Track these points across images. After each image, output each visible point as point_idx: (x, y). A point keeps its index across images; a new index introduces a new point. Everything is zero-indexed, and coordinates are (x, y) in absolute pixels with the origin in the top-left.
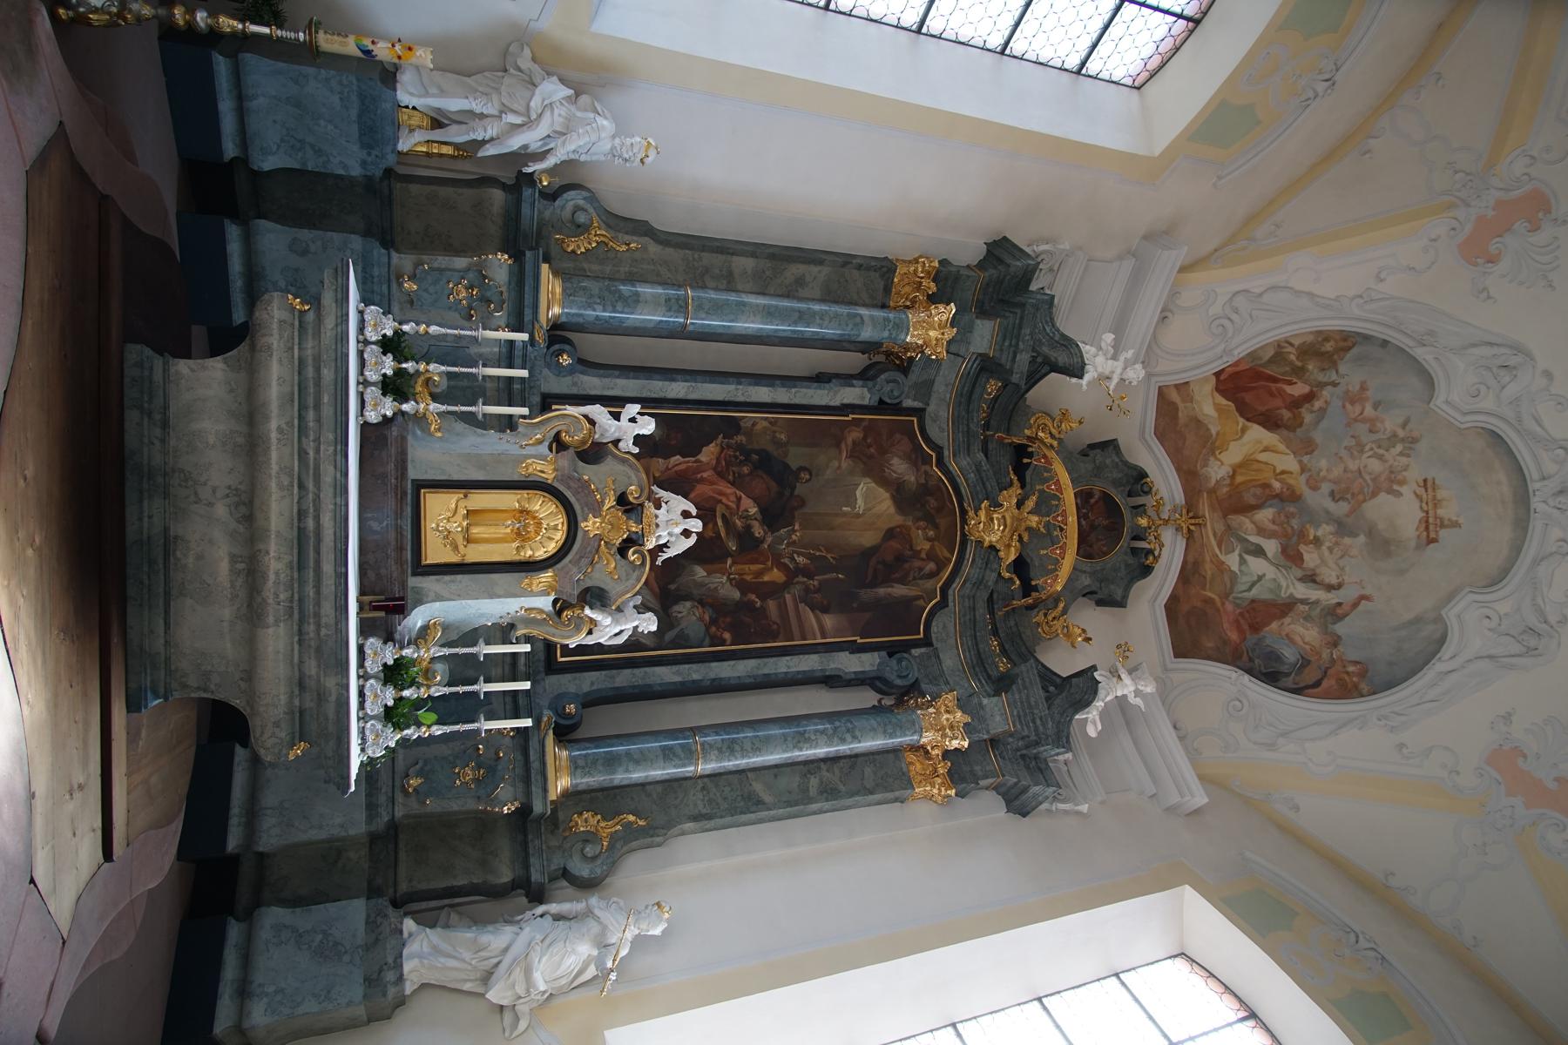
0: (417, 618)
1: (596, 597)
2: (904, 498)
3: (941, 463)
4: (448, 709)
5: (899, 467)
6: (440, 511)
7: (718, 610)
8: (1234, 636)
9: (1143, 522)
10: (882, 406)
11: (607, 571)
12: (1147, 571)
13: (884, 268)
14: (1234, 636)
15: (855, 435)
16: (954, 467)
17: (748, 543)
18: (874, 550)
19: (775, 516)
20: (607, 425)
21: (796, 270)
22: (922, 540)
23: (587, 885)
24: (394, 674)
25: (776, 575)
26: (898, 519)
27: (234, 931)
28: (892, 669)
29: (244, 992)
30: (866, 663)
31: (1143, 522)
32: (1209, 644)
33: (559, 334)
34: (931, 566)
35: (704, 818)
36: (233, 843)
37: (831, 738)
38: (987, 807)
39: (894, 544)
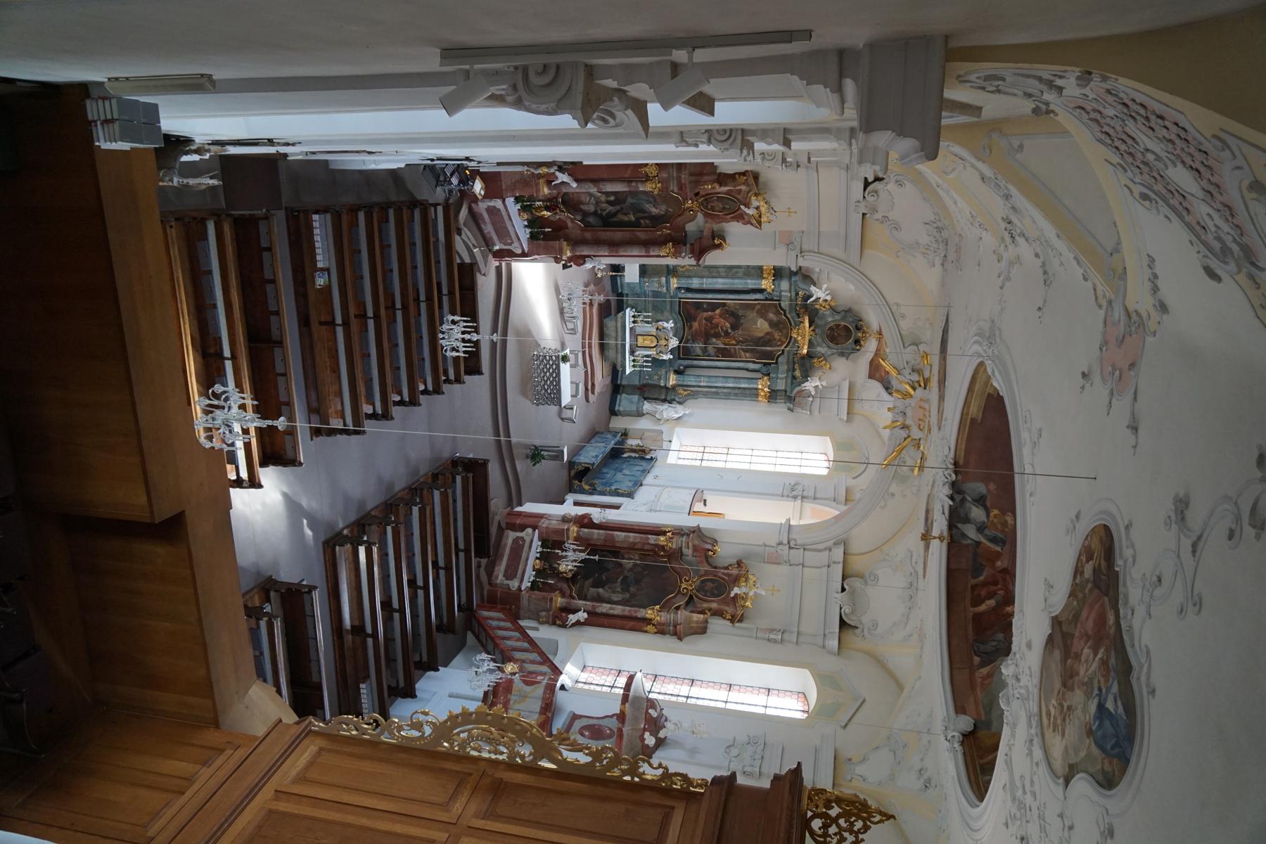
0: (637, 353)
1: (662, 353)
2: (772, 324)
3: (785, 315)
4: (641, 366)
5: (771, 316)
6: (640, 339)
7: (719, 349)
8: (883, 374)
9: (860, 335)
10: (766, 299)
11: (663, 349)
12: (858, 350)
13: (760, 268)
14: (883, 374)
15: (759, 307)
16: (789, 316)
17: (727, 334)
18: (762, 337)
19: (734, 327)
20: (665, 325)
21: (735, 270)
22: (777, 335)
23: (680, 403)
24: (634, 361)
25: (734, 342)
26: (770, 330)
27: (619, 396)
28: (764, 370)
29: (619, 405)
30: (756, 366)
31: (860, 335)
32: (878, 375)
33: (679, 288)
34: (779, 343)
35: (706, 395)
36: (619, 382)
37: (733, 383)
38: (781, 408)
39: (768, 337)
